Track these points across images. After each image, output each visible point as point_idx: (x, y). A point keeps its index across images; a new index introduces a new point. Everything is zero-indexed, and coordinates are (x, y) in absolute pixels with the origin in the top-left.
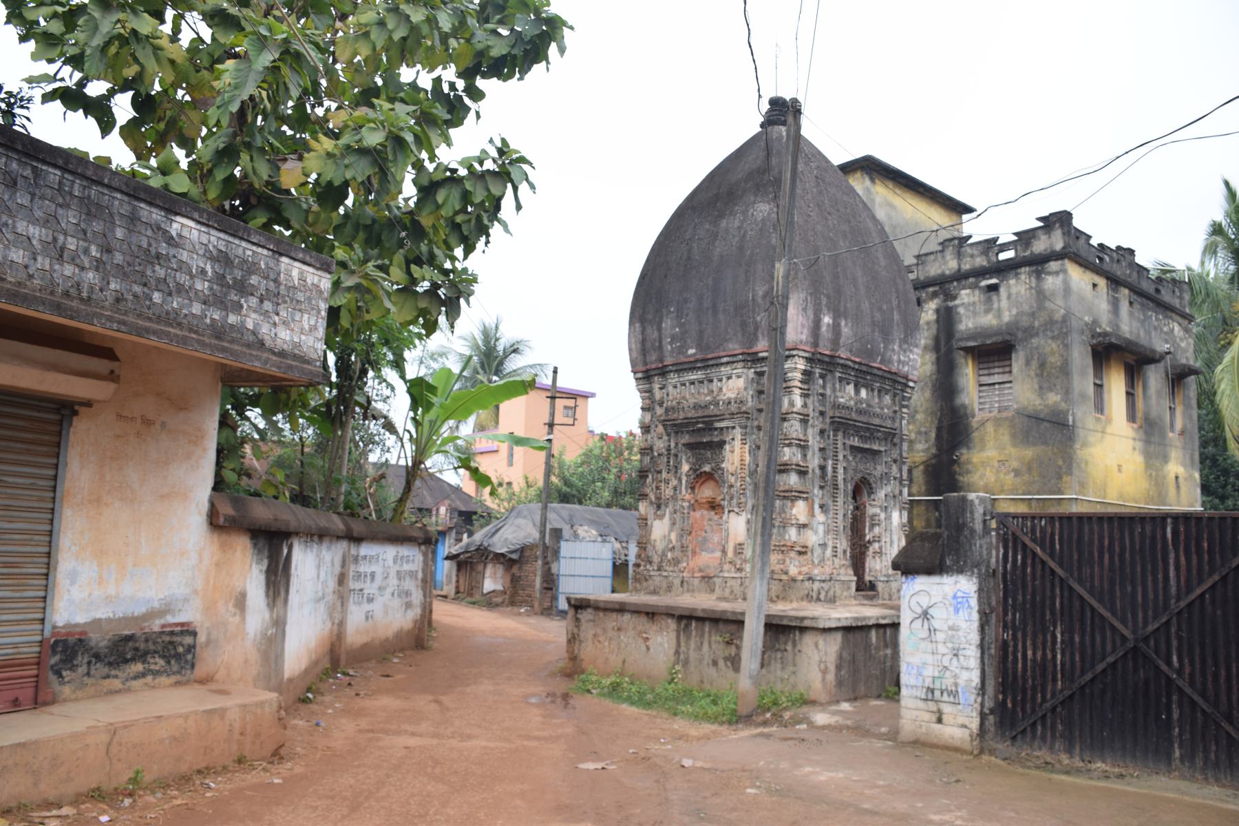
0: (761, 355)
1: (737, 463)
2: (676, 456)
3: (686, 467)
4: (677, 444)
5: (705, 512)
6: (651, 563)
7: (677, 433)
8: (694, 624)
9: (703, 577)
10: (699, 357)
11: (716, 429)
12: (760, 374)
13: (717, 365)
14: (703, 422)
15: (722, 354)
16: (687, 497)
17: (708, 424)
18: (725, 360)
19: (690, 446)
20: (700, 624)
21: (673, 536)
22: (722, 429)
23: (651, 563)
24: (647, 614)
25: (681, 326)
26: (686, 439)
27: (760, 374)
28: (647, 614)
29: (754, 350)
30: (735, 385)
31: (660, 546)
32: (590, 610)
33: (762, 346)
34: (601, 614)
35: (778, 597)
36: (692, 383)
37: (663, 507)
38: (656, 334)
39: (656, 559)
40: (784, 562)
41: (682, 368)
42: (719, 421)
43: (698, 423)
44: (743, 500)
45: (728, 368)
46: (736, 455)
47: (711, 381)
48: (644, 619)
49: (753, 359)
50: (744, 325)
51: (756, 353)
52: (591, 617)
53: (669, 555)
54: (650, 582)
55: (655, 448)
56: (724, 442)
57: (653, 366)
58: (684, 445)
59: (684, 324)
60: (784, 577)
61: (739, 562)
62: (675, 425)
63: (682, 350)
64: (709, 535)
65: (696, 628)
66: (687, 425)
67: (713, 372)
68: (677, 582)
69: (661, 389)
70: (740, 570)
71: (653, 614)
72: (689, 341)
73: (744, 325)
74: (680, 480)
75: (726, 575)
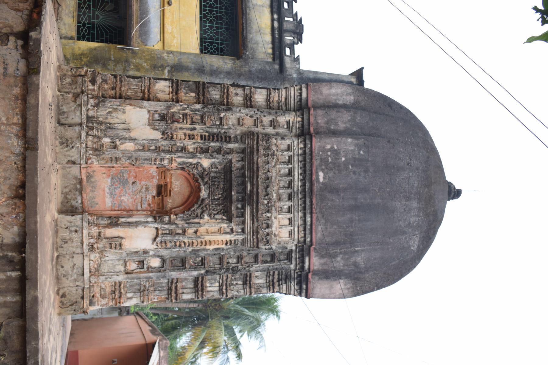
0: (307, 260)
1: (208, 238)
2: (219, 151)
3: (206, 163)
4: (231, 151)
5: (155, 182)
6: (97, 105)
7: (243, 151)
8: (14, 274)
9: (81, 182)
10: (316, 186)
11: (243, 207)
12: (289, 256)
13: (304, 209)
14: (252, 191)
15: (314, 216)
16: (174, 165)
17: (250, 199)
18: (308, 219)
19: (228, 169)
20: (15, 285)
21: (129, 146)
22: (243, 215)
23: (97, 105)
24: (23, 186)
25: (346, 164)
26: (236, 165)
27: (289, 257)
28: (23, 186)
29: (313, 253)
30: (283, 229)
31: (117, 119)
32: (22, 65)
33: (315, 262)
34: (17, 91)
35: (63, 296)
36: (290, 173)
37: (162, 125)
38: (342, 126)
39: (101, 113)
40: (103, 297)
41: (307, 159)
42: (252, 212)
43: (252, 185)
44: (169, 245)
45: (300, 222)
46: (214, 234)
47: (290, 198)
48: (14, 178)
49: (304, 250)
50: (337, 244)
51: (309, 255)
52: (11, 70)
53: (106, 140)
54: (73, 106)
55: (229, 114)
56: (230, 220)
57: (312, 119)
58: (230, 162)
59: (347, 168)
60: (86, 302)
61: (100, 245)
62: (252, 152)
63: (326, 166)
64: (131, 189)
65: (9, 278)
66: (251, 169)
67: (297, 202)
68: (74, 154)
69: (288, 123)
70: (92, 248)
71: (22, 197)
72: (331, 174)
73: (337, 244)
74: (194, 156)
75: (85, 232)
